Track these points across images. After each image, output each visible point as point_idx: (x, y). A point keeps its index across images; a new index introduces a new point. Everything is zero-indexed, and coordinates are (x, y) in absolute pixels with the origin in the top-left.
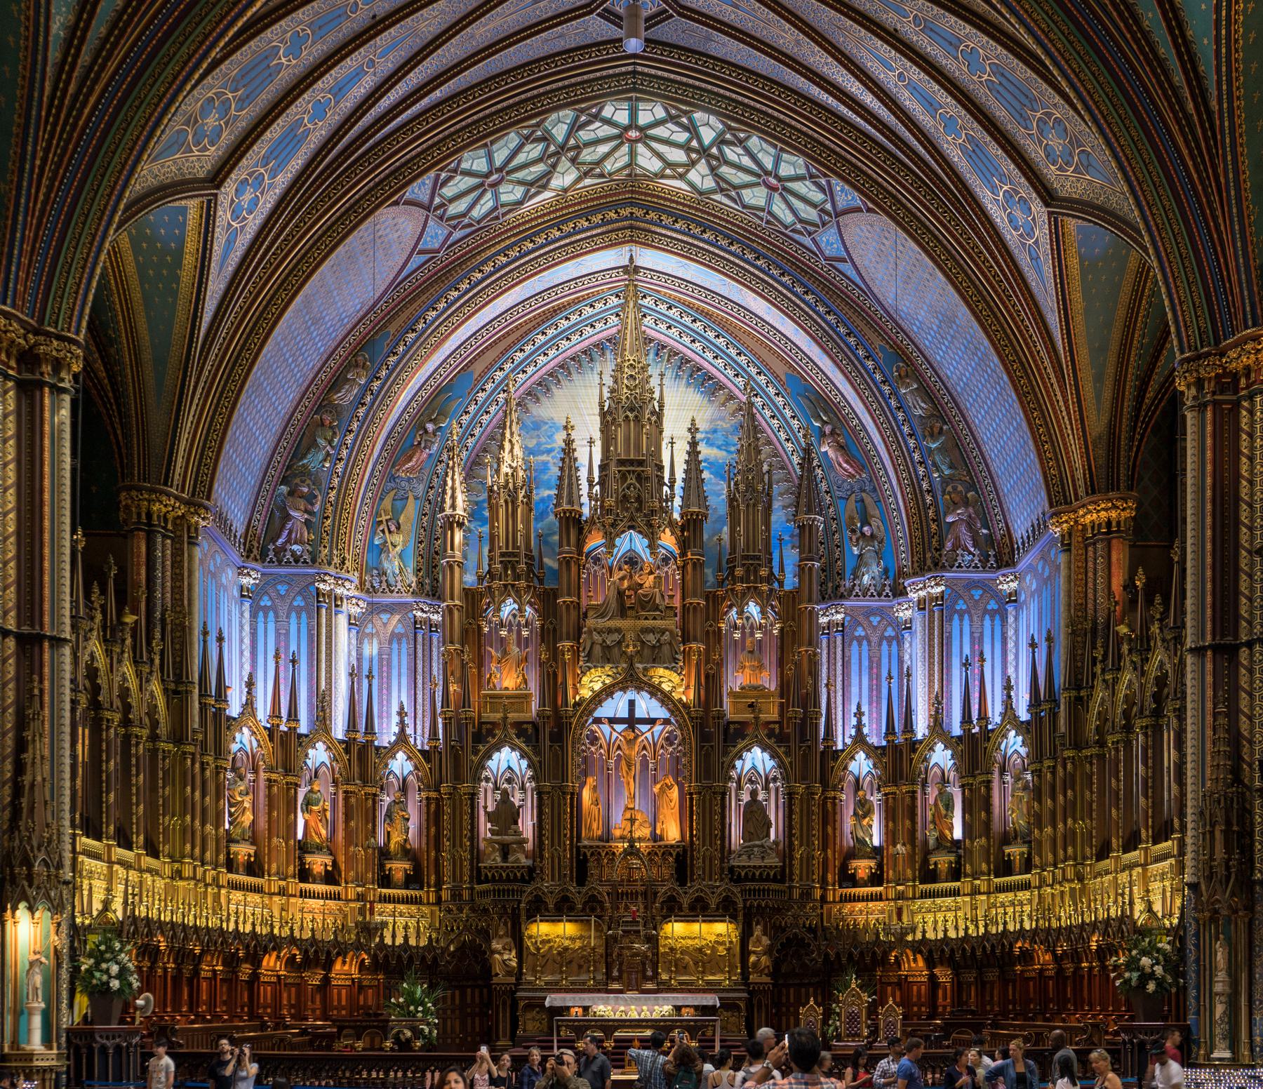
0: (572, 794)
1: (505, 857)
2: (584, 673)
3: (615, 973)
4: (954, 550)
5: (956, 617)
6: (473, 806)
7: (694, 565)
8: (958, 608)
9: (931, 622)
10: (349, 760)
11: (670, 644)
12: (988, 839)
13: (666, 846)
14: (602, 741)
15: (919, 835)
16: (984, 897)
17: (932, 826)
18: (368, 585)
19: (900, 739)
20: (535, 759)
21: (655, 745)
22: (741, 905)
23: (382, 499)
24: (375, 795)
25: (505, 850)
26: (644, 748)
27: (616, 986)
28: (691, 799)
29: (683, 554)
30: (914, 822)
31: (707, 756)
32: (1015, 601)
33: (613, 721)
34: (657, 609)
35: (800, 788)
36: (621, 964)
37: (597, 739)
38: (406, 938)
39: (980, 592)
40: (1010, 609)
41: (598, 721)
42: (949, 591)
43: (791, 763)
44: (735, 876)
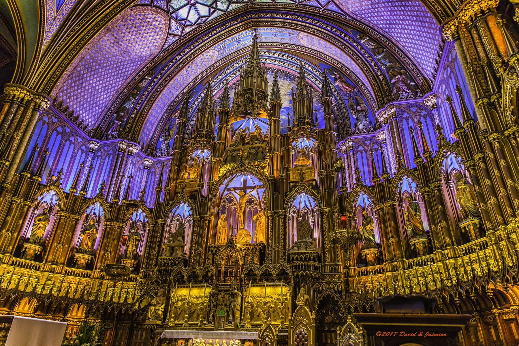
0: (209, 221)
1: (171, 254)
2: (221, 168)
3: (211, 318)
4: (397, 92)
5: (404, 120)
6: (163, 230)
7: (275, 122)
8: (404, 116)
9: (392, 127)
10: (111, 211)
11: (262, 152)
12: (446, 220)
13: (254, 245)
14: (235, 202)
15: (401, 229)
16: (452, 261)
17: (408, 223)
18: (154, 154)
19: (382, 179)
20: (194, 206)
21: (260, 202)
22: (290, 275)
23: (165, 126)
24: (122, 227)
25: (172, 250)
26: (256, 204)
27: (209, 327)
28: (268, 219)
29: (270, 119)
30: (396, 223)
31: (277, 198)
32: (437, 107)
33: (235, 189)
34: (258, 140)
35: (327, 210)
36: (215, 312)
37: (233, 201)
38: (112, 297)
39: (416, 108)
40: (435, 112)
41: (229, 189)
42: (398, 110)
43: (321, 197)
44: (289, 259)
